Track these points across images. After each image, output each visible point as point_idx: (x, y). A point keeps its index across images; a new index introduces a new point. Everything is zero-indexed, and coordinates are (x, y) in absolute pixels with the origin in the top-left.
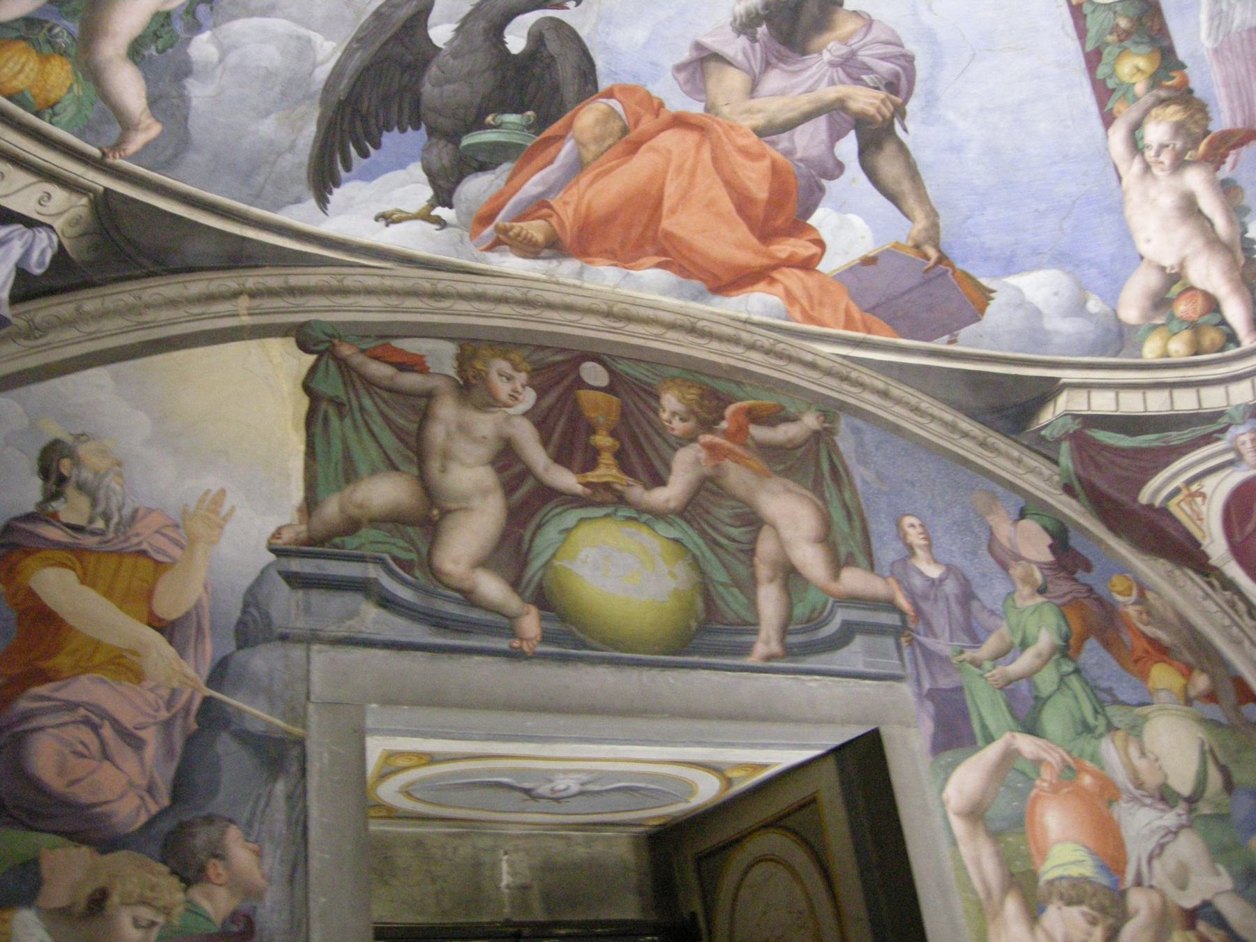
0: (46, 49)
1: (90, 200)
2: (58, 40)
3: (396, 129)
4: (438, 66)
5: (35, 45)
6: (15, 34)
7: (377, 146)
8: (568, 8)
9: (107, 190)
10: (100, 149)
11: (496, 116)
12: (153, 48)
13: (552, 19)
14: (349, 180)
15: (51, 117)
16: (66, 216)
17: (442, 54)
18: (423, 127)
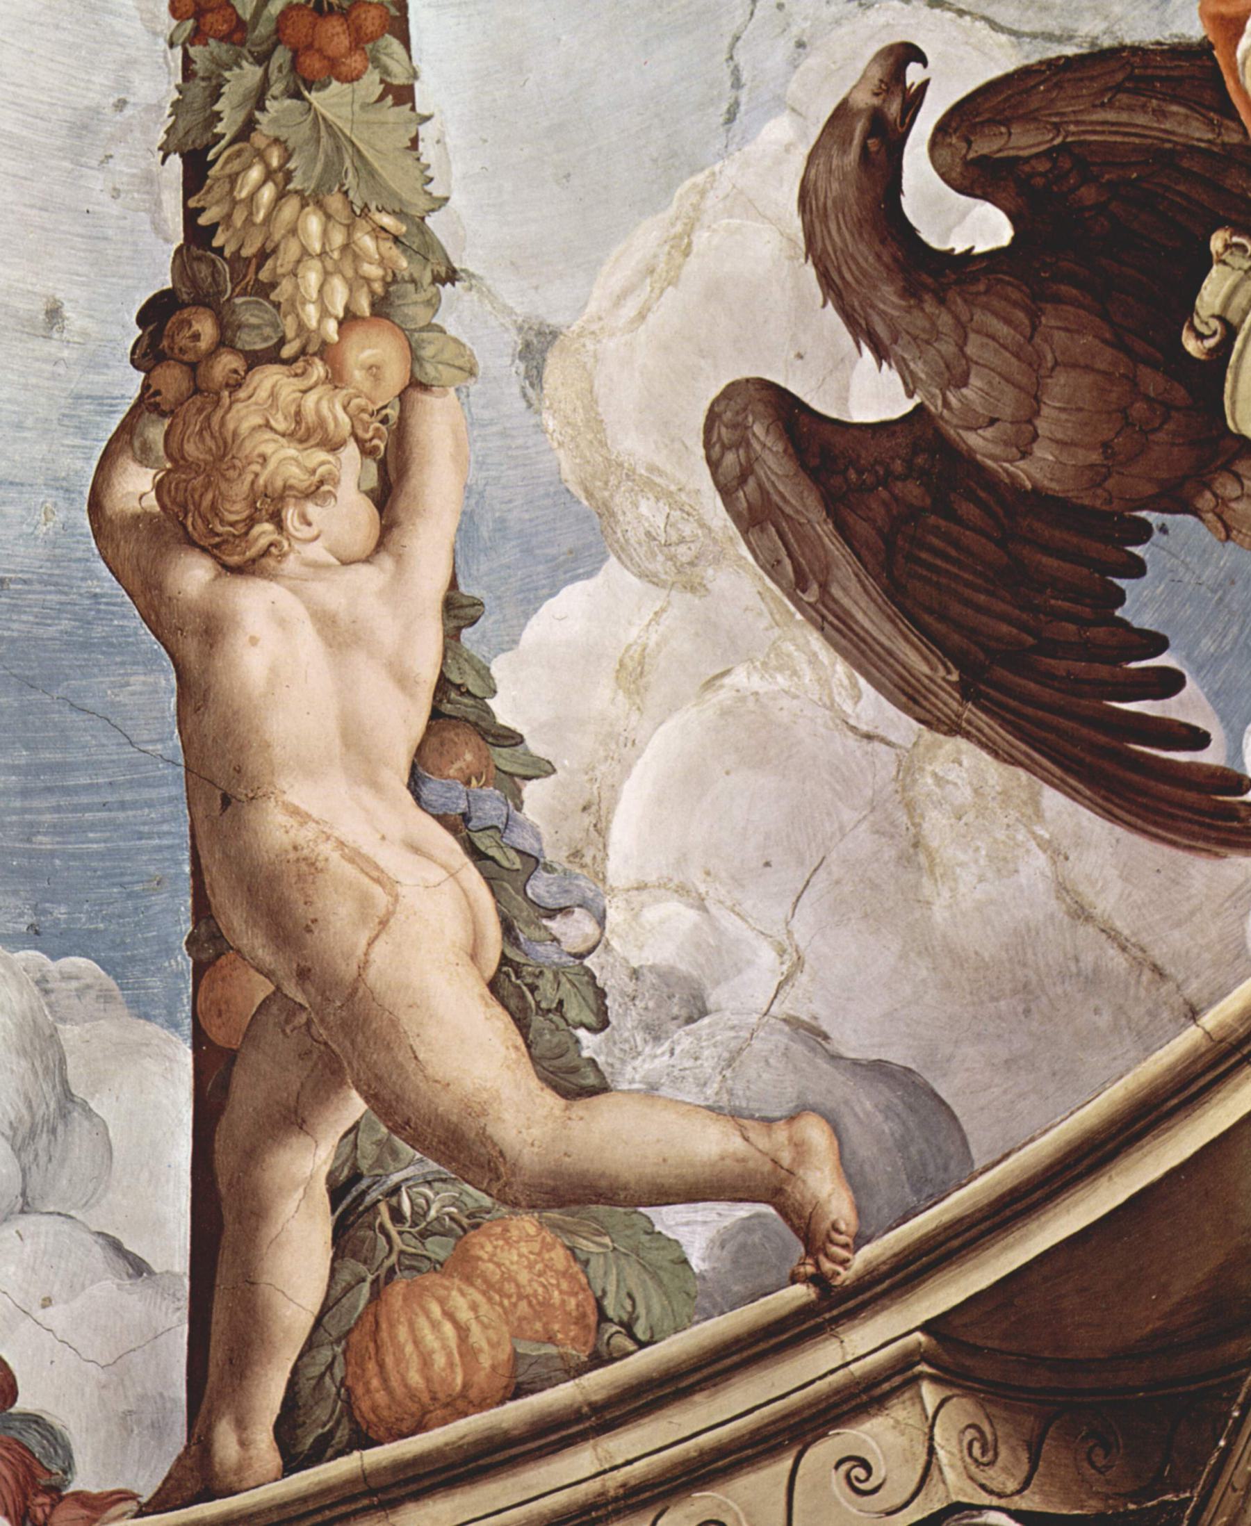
0: (437, 1248)
1: (934, 1379)
2: (433, 1213)
3: (1122, 583)
4: (969, 428)
5: (413, 1264)
6: (366, 1289)
7: (1158, 644)
8: (924, 85)
9: (927, 1327)
10: (794, 1280)
11: (1192, 328)
12: (582, 1033)
13: (942, 129)
14: (1237, 751)
15: (632, 1336)
16: (941, 1453)
17: (936, 407)
18: (1143, 514)
